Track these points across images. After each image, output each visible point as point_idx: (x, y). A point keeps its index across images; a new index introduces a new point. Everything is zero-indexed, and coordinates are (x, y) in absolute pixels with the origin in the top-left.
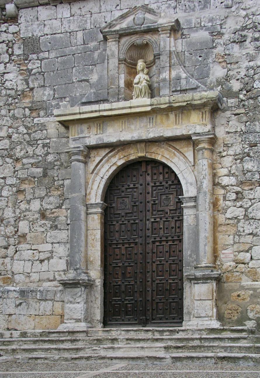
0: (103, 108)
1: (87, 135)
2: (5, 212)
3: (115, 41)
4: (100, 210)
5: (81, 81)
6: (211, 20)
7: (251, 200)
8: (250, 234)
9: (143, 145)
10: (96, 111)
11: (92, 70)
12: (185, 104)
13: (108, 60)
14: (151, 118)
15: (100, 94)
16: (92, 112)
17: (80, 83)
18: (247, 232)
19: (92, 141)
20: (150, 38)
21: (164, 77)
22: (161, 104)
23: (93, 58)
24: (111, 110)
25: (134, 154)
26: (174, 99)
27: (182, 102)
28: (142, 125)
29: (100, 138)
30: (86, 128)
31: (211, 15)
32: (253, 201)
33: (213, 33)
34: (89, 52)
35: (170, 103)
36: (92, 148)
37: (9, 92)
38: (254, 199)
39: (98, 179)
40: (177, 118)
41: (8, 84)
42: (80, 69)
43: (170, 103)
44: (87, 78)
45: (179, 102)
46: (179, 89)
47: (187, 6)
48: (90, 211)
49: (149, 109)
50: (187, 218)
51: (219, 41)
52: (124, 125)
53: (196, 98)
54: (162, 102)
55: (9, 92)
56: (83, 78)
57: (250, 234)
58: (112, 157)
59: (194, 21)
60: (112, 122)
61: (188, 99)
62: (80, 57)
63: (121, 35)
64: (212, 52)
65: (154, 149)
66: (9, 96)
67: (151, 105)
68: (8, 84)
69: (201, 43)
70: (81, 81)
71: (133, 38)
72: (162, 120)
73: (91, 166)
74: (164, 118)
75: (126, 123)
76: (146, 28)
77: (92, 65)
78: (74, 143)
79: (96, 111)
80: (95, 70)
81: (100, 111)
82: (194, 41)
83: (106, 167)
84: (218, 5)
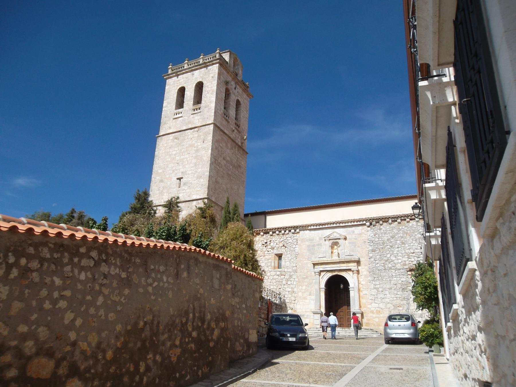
2: (295, 289)
4: (324, 290)
19: (322, 269)
36: (321, 271)
37: (296, 253)
39: (323, 281)
41: (296, 251)
48: (321, 290)
49: (338, 261)
55: (296, 253)
66: (296, 254)
68: (296, 251)
73: (321, 276)
83: (326, 276)
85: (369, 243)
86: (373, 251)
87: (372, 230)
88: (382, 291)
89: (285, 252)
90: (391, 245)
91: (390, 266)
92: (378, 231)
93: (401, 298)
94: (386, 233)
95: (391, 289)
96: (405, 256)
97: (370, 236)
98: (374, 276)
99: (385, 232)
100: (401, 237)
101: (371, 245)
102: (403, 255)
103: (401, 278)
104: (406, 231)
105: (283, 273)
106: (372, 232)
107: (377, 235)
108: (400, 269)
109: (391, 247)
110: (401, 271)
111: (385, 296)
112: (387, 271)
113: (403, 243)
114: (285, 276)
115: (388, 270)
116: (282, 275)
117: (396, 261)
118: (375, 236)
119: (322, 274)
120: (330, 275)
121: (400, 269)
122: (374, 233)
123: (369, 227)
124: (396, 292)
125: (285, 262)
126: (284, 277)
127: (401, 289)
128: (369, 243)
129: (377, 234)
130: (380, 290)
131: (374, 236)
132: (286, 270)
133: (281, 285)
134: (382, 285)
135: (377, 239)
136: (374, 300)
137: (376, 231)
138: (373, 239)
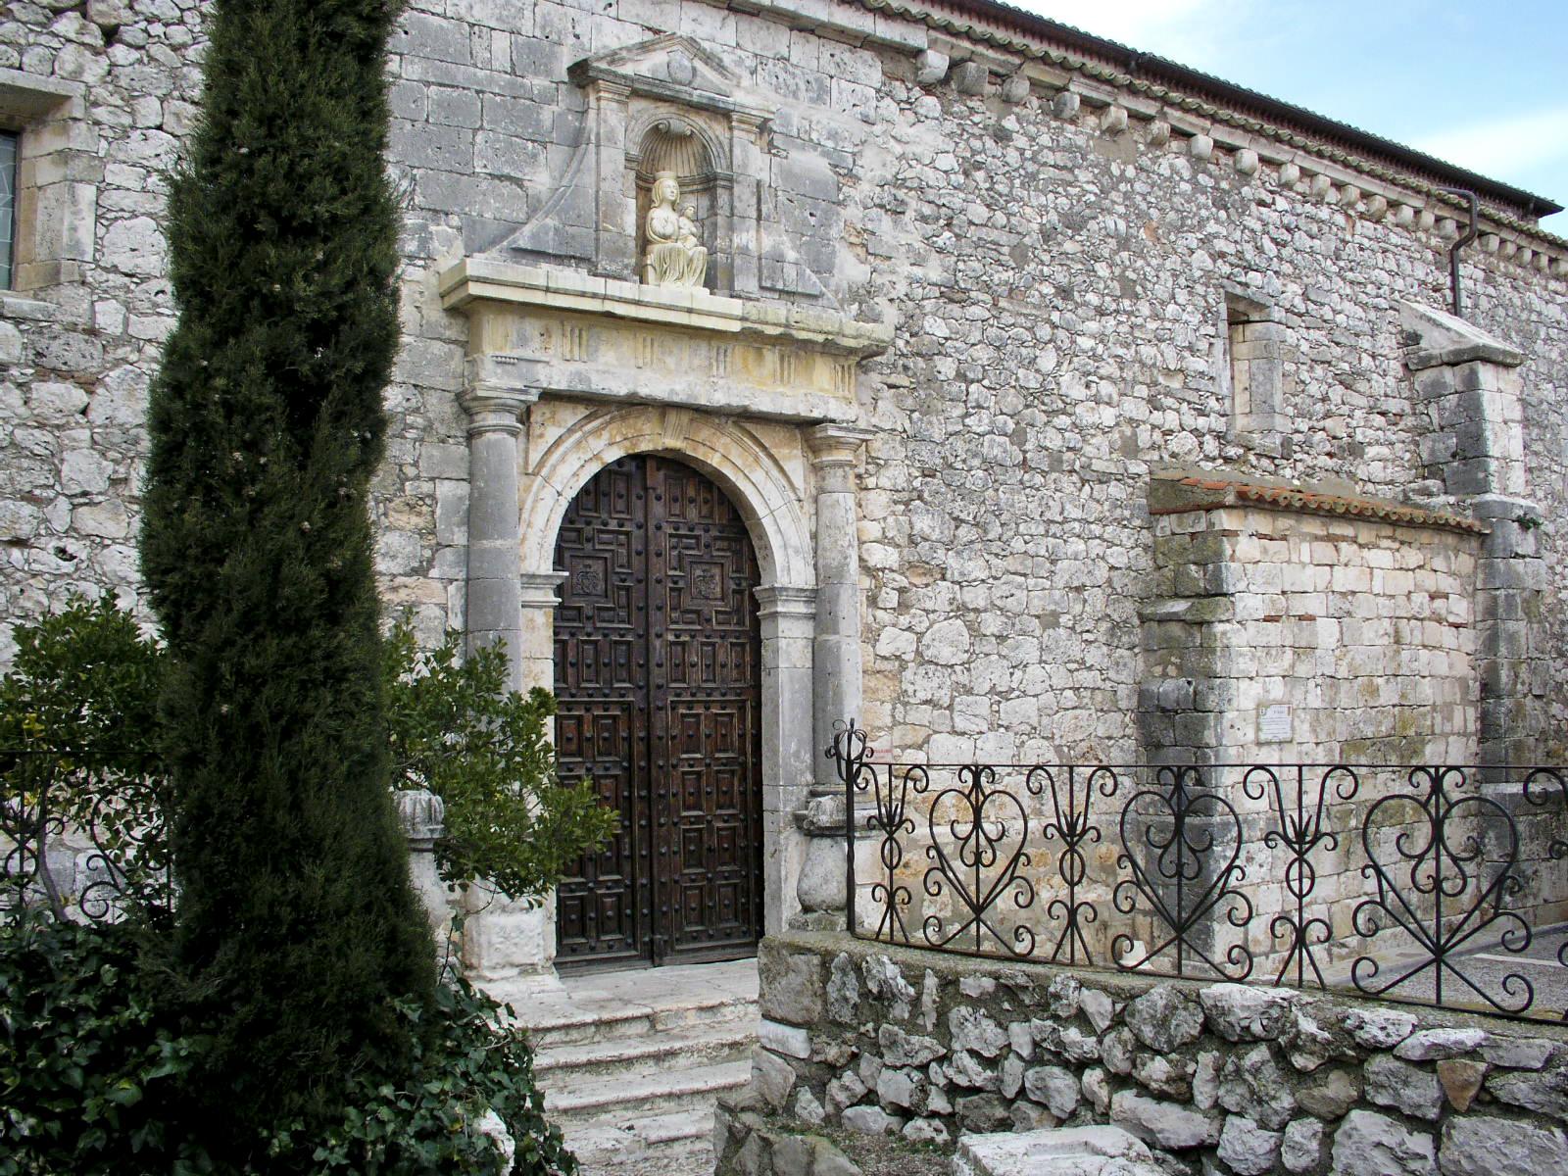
0: (617, 294)
1: (538, 356)
3: (618, 102)
5: (500, 178)
6: (833, 135)
7: (927, 612)
8: (926, 702)
9: (685, 418)
10: (594, 296)
11: (535, 156)
12: (820, 338)
13: (598, 146)
14: (722, 351)
15: (573, 237)
16: (583, 294)
17: (497, 182)
18: (922, 695)
19: (558, 376)
20: (704, 126)
21: (744, 242)
22: (767, 323)
23: (538, 121)
24: (638, 303)
25: (653, 438)
26: (797, 317)
27: (814, 331)
28: (696, 362)
29: (579, 373)
30: (537, 333)
31: (832, 124)
32: (931, 616)
33: (836, 166)
34: (528, 102)
35: (787, 326)
36: (549, 396)
38: (934, 611)
39: (548, 494)
40: (786, 365)
42: (499, 141)
43: (787, 326)
44: (520, 175)
45: (809, 330)
46: (780, 286)
47: (781, 80)
49: (735, 327)
50: (788, 645)
51: (852, 192)
52: (648, 350)
53: (847, 332)
54: (770, 318)
56: (506, 170)
57: (926, 702)
58: (597, 432)
59: (795, 121)
60: (615, 333)
61: (830, 328)
62: (499, 105)
63: (639, 91)
64: (838, 214)
65: (705, 433)
67: (743, 319)
69: (813, 182)
70: (500, 178)
71: (662, 110)
72: (745, 359)
74: (751, 356)
75: (584, 333)
76: (705, 101)
77: (533, 141)
78: (499, 371)
79: (594, 296)
80: (542, 158)
81: (605, 298)
82: (797, 170)
83: (573, 462)
84: (849, 106)
85: (924, 219)
86: (952, 294)
87: (950, 125)
88: (1001, 638)
89: (101, 92)
90: (1062, 278)
91: (1054, 441)
92: (990, 143)
93: (1099, 696)
94: (1033, 176)
95: (1050, 620)
96: (1135, 382)
97: (932, 164)
98: (957, 507)
99: (1031, 167)
100: (1116, 235)
101: (940, 242)
102: (1128, 375)
103: (1111, 544)
104: (1144, 206)
105: (74, 352)
106: (951, 135)
107: (980, 175)
108: (1104, 479)
109: (1065, 292)
110: (1115, 490)
111: (1018, 674)
112: (1038, 479)
113: (1129, 290)
114: (89, 385)
115: (1044, 473)
116: (45, 373)
117: (1086, 414)
118: (966, 174)
119: (553, 427)
120: (607, 447)
121: (1104, 479)
122: (963, 151)
123: (928, 89)
124: (1076, 649)
125: (103, 216)
126: (79, 397)
127: (1104, 626)
128: (924, 219)
129: (978, 166)
130: (992, 623)
131: (961, 179)
132: (109, 315)
133: (29, 498)
134: (1005, 590)
135: (979, 212)
136: (950, 707)
137: (977, 144)
138: (957, 201)
